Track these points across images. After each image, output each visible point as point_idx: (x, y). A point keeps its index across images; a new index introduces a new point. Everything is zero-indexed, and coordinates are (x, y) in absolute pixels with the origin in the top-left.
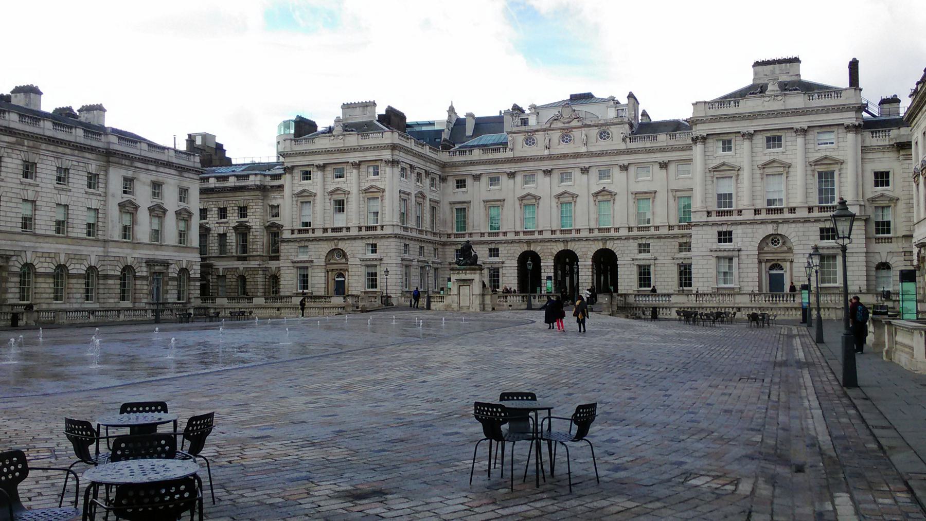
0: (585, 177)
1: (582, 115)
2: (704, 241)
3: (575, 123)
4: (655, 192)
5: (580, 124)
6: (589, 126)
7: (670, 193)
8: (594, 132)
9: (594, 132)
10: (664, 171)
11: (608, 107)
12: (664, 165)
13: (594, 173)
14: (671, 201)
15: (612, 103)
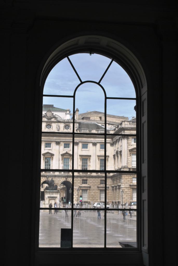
0: (58, 146)
1: (56, 116)
2: (127, 181)
3: (53, 120)
4: (90, 156)
5: (55, 121)
6: (59, 122)
7: (97, 157)
8: (62, 125)
9: (62, 125)
10: (94, 147)
11: (66, 114)
12: (94, 144)
13: (62, 144)
14: (97, 160)
15: (68, 112)
